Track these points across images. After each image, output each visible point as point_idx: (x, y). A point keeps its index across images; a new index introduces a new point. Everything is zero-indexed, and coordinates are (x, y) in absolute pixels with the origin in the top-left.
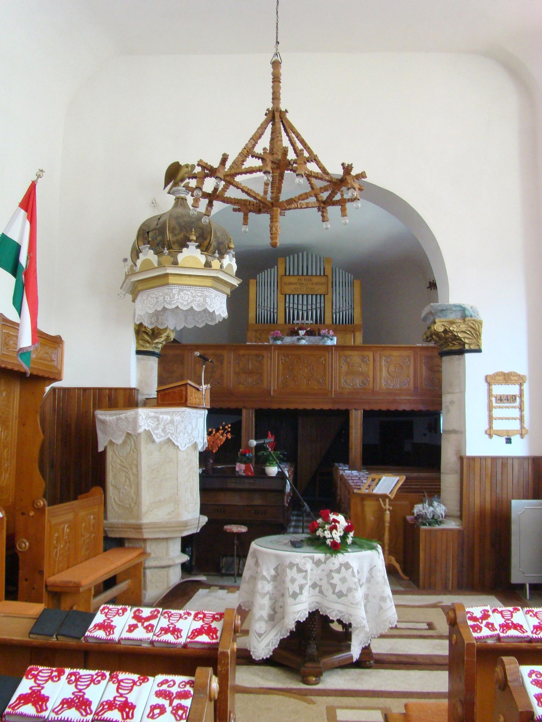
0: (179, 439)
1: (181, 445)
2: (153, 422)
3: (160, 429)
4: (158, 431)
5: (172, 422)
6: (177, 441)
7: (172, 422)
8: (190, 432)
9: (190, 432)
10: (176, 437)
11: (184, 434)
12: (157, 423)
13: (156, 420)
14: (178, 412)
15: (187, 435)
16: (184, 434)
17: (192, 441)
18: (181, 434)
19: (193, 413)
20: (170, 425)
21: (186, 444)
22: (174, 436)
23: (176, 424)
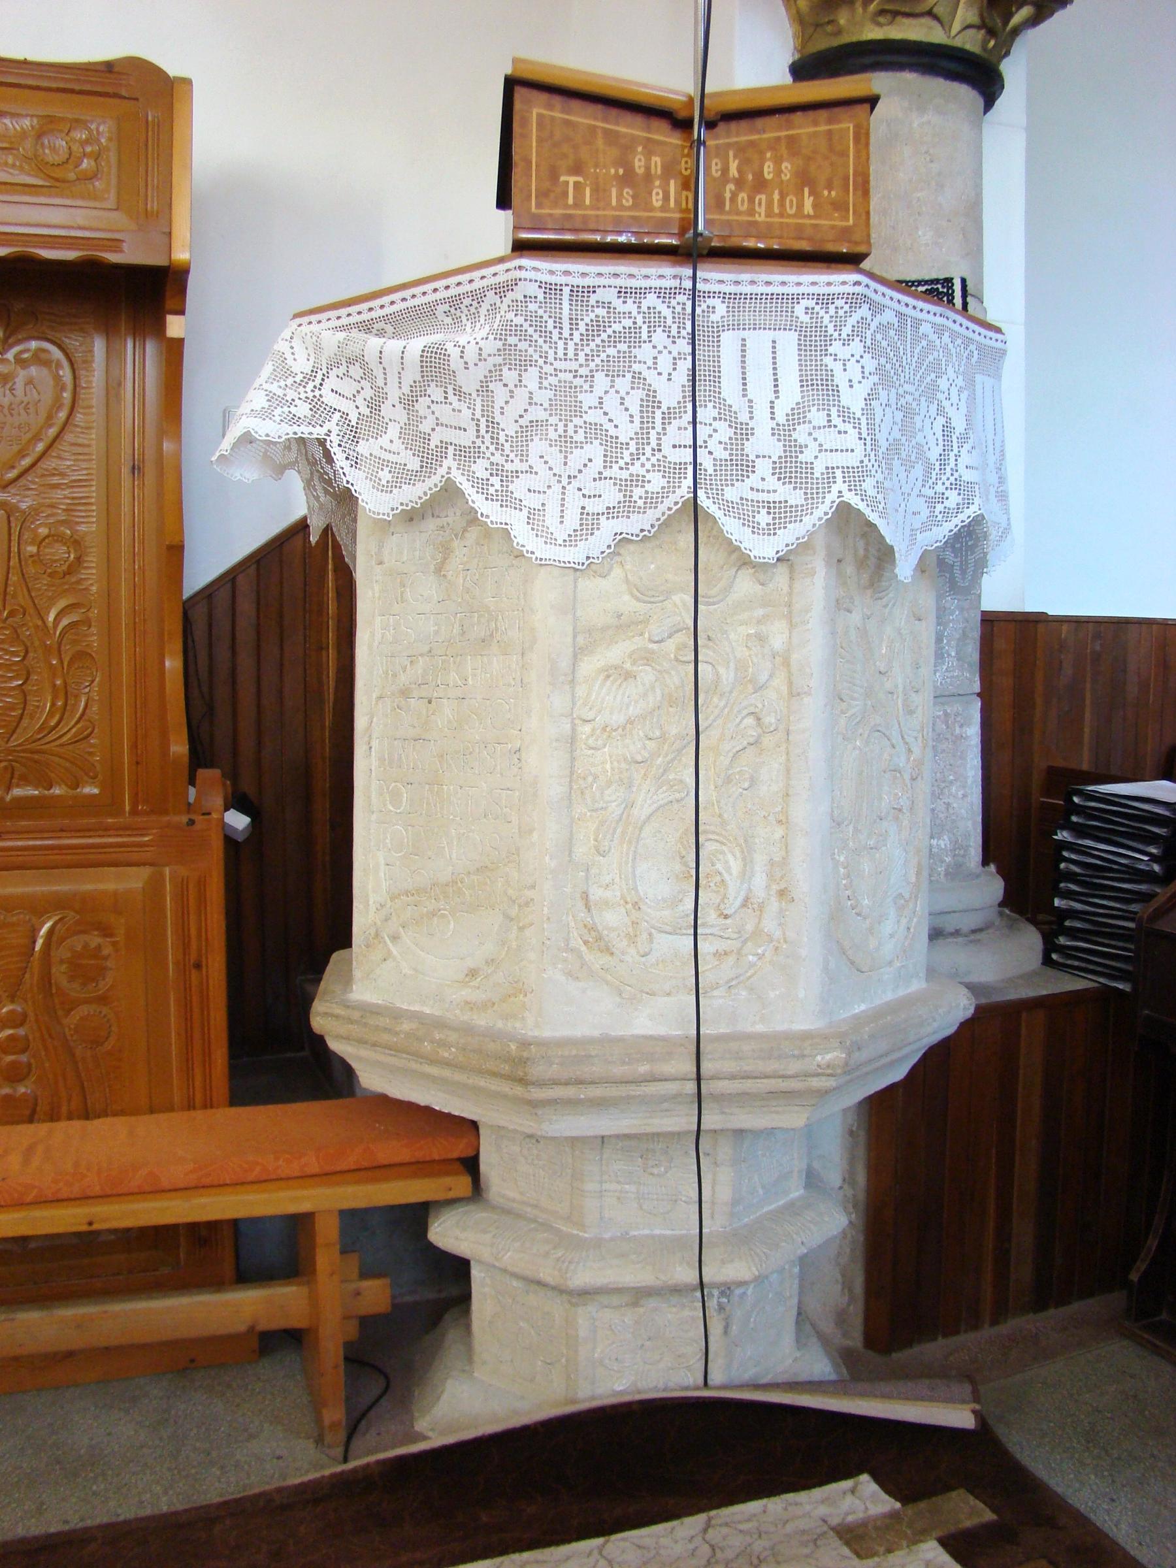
0: (519, 487)
1: (534, 517)
2: (348, 387)
3: (393, 431)
4: (384, 441)
5: (434, 365)
6: (506, 499)
7: (434, 365)
8: (626, 431)
9: (626, 431)
10: (496, 470)
11: (566, 443)
12: (368, 393)
13: (356, 371)
14: (478, 297)
15: (595, 451)
16: (566, 443)
17: (652, 501)
18: (537, 447)
19: (622, 293)
20: (436, 393)
21: (588, 523)
22: (480, 469)
23: (469, 381)
